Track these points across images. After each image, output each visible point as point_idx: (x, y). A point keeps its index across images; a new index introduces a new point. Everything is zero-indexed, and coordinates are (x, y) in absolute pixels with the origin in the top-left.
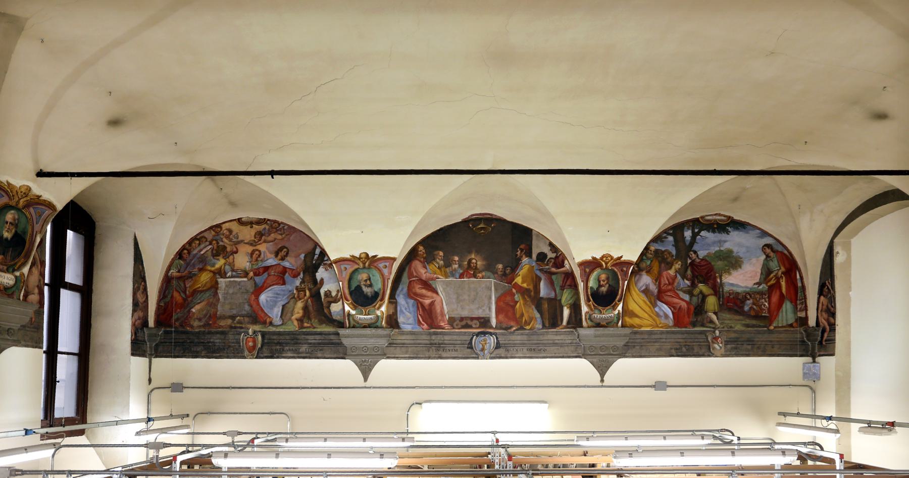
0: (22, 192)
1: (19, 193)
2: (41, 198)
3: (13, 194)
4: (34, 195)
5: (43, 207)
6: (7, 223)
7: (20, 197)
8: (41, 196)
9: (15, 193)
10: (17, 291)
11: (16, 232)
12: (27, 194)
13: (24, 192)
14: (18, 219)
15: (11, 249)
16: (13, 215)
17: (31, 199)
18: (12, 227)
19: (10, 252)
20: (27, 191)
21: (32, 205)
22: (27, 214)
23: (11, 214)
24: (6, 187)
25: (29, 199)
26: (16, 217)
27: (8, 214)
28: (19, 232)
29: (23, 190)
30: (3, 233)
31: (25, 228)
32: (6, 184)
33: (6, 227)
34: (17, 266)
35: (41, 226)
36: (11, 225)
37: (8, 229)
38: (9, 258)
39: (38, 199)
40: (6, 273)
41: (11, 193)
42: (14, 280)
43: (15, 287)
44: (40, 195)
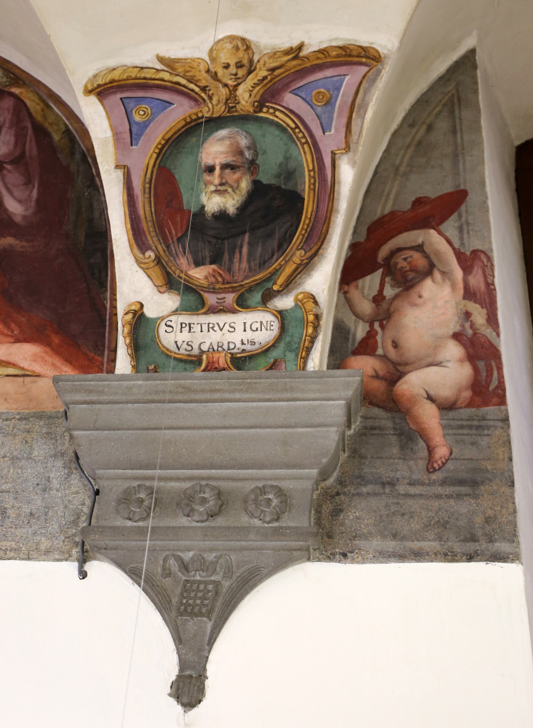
0: (227, 66)
1: (221, 72)
2: (304, 52)
3: (203, 84)
4: (274, 54)
5: (329, 73)
6: (211, 169)
7: (231, 83)
8: (300, 47)
9: (205, 79)
10: (290, 356)
11: (256, 183)
12: (245, 62)
13: (232, 62)
14: (253, 147)
15: (247, 237)
16: (227, 142)
17: (273, 70)
18: (231, 177)
19: (245, 250)
20: (241, 54)
21: (287, 86)
22: (281, 118)
23: (222, 139)
24: (166, 76)
25: (264, 73)
26: (244, 142)
27: (206, 145)
28: (265, 179)
29: (225, 57)
30: (199, 200)
31: (287, 159)
32: (159, 66)
33: (207, 184)
34: (281, 280)
35: (344, 129)
36: (228, 171)
37: (221, 184)
38: (244, 265)
39: (296, 57)
40: (234, 311)
41: (192, 86)
42: (276, 326)
43: (282, 346)
44: (295, 43)
